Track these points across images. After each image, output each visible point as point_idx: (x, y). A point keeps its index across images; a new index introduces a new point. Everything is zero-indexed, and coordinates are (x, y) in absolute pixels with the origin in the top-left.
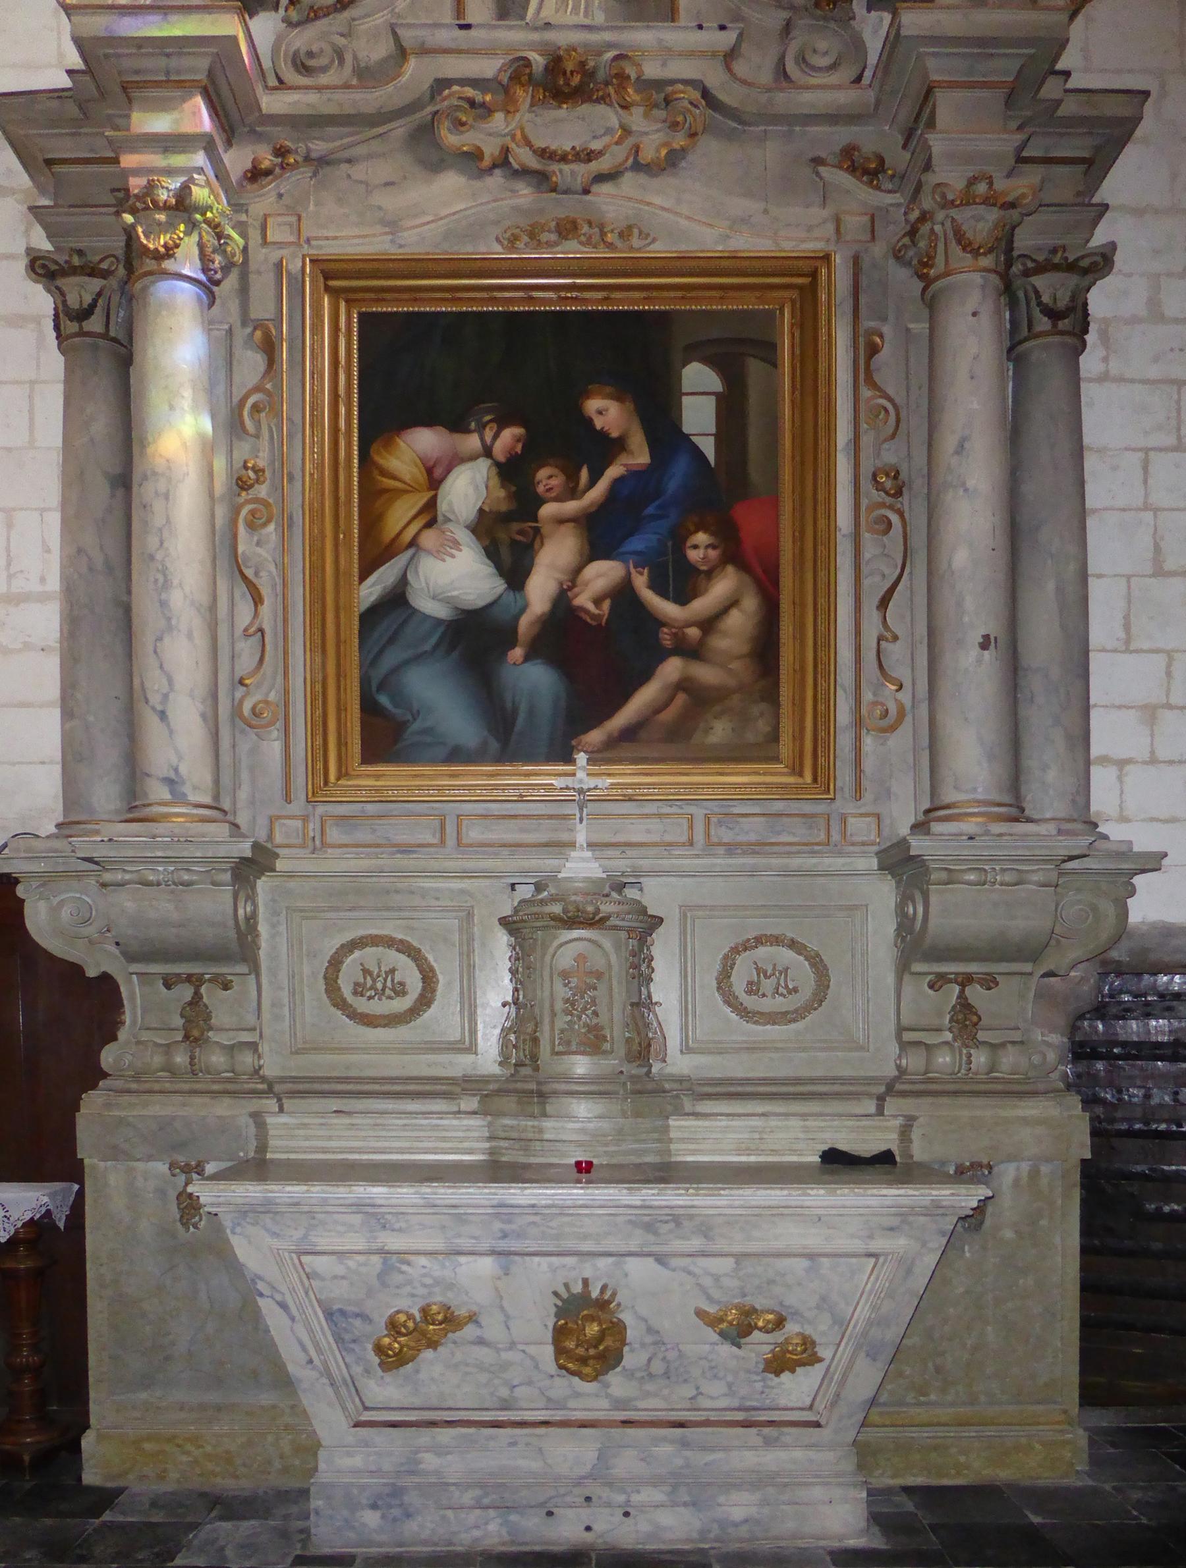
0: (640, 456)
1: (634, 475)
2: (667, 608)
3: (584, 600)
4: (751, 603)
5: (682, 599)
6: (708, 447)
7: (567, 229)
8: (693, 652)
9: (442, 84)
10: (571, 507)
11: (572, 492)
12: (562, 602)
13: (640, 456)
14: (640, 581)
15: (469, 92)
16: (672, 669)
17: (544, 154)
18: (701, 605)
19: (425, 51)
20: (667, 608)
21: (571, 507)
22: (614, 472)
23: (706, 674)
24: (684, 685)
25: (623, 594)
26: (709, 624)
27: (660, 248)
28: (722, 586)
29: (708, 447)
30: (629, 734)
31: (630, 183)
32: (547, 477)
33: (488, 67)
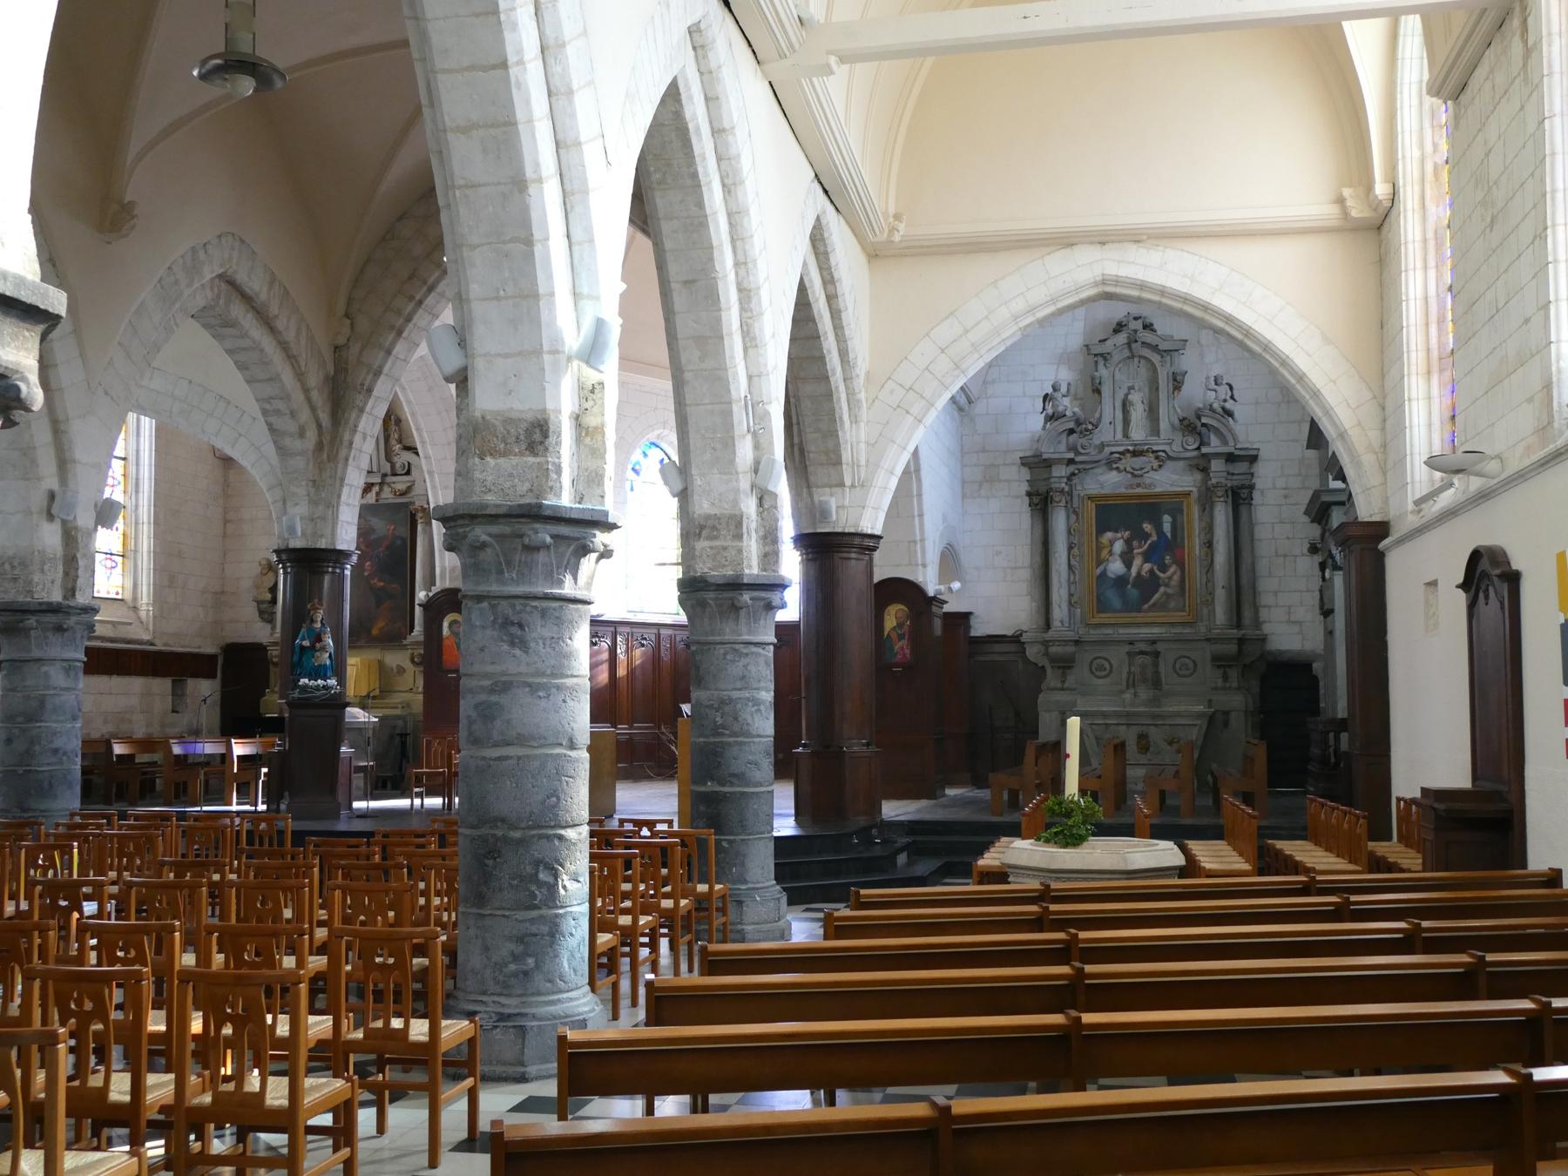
0: (1154, 538)
1: (1153, 542)
2: (1161, 575)
3: (1143, 573)
4: (1179, 573)
5: (1164, 573)
6: (1169, 535)
7: (1138, 485)
8: (1167, 585)
9: (1112, 453)
10: (1140, 550)
11: (1140, 547)
12: (1139, 573)
13: (1154, 538)
14: (1155, 568)
15: (1117, 455)
16: (1162, 589)
17: (1133, 469)
18: (1169, 573)
19: (1108, 445)
20: (1161, 575)
21: (1140, 550)
22: (1149, 542)
23: (1170, 591)
24: (1165, 593)
25: (1151, 571)
26: (1170, 578)
27: (1158, 490)
28: (1172, 569)
29: (1169, 535)
30: (1154, 605)
31: (1152, 474)
32: (1135, 543)
33: (1121, 449)
